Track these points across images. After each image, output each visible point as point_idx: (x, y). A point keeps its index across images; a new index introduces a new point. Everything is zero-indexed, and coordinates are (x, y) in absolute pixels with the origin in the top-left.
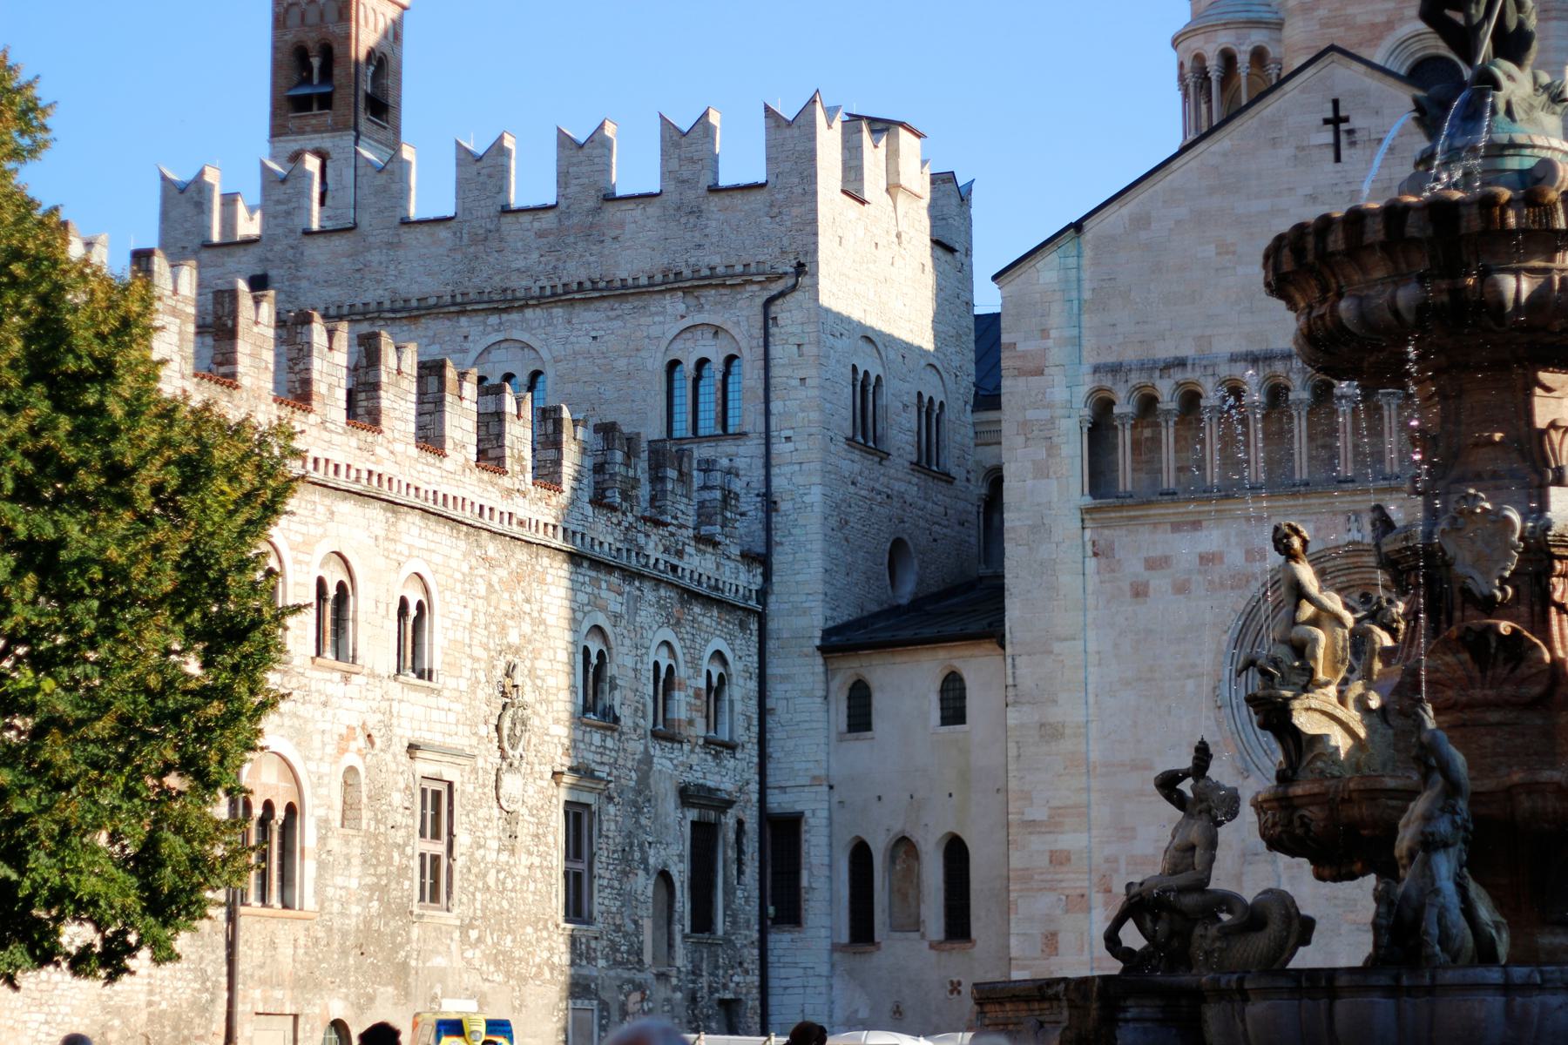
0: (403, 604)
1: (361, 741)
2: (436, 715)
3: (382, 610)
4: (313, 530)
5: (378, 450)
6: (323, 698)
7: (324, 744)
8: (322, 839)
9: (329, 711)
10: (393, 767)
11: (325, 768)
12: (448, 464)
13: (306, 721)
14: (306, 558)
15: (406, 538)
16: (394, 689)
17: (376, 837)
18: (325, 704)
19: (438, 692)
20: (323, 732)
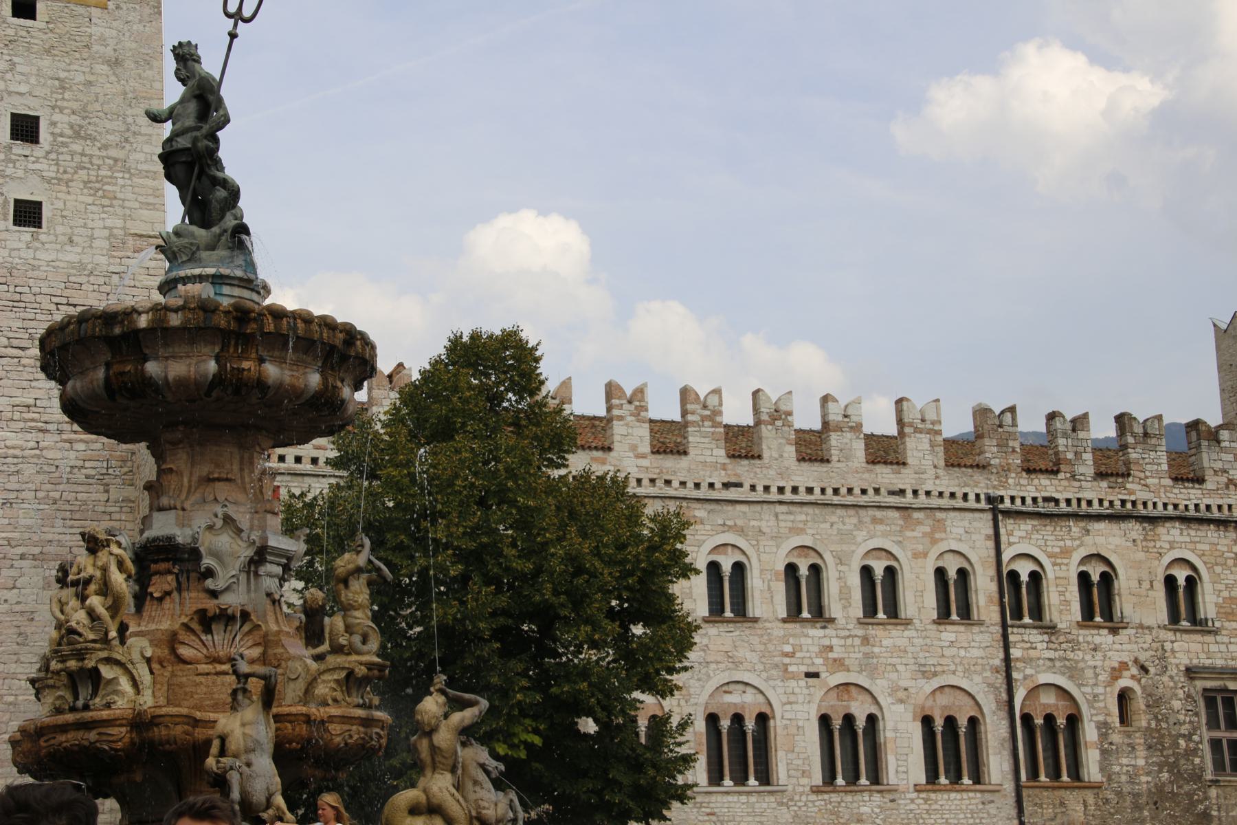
0: (1170, 581)
1: (1134, 670)
2: (1213, 648)
3: (1146, 585)
4: (1069, 543)
5: (1128, 486)
6: (1092, 646)
7: (1096, 675)
8: (1103, 736)
9: (1099, 655)
10: (1172, 684)
11: (1100, 690)
12: (1209, 485)
13: (1077, 662)
14: (1065, 561)
15: (1164, 538)
16: (1164, 635)
17: (1158, 731)
18: (1095, 650)
19: (1215, 632)
20: (1095, 667)
